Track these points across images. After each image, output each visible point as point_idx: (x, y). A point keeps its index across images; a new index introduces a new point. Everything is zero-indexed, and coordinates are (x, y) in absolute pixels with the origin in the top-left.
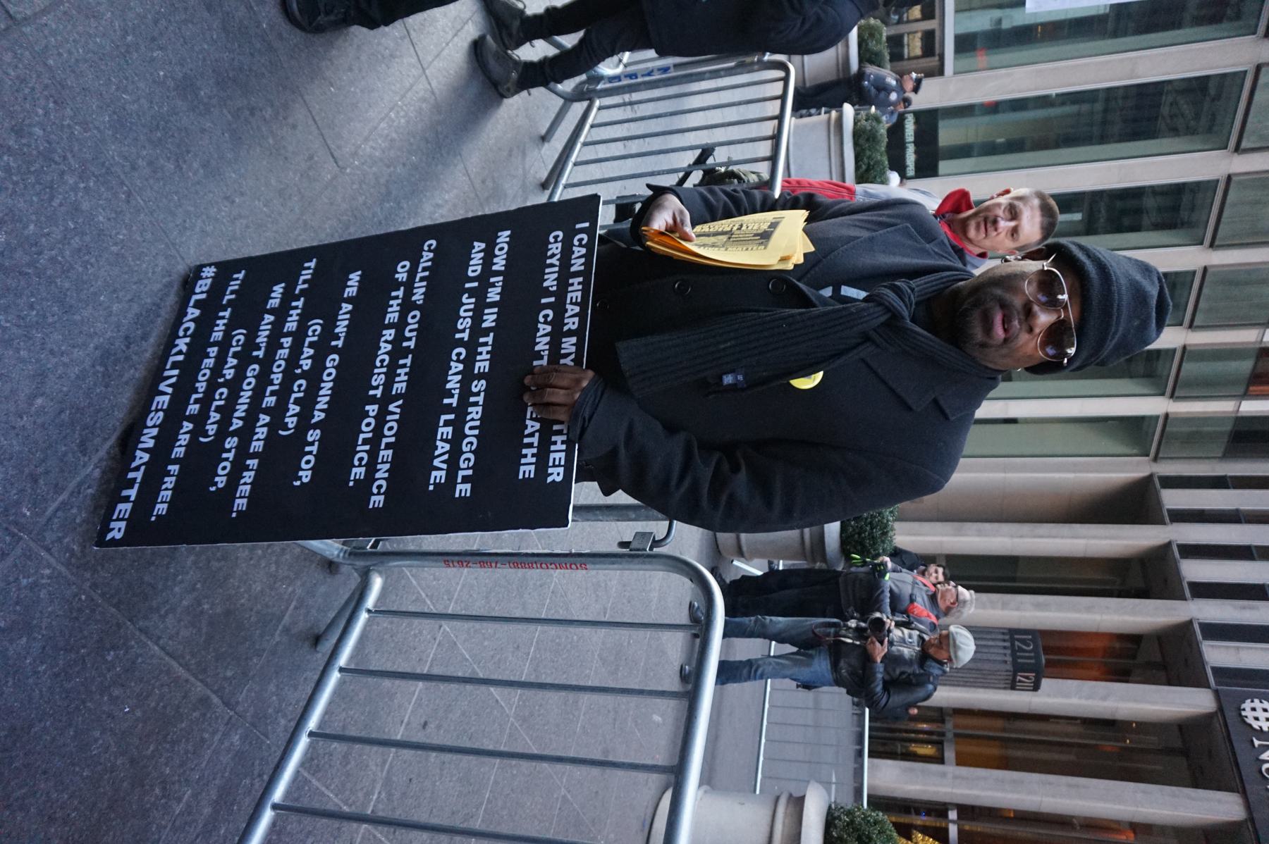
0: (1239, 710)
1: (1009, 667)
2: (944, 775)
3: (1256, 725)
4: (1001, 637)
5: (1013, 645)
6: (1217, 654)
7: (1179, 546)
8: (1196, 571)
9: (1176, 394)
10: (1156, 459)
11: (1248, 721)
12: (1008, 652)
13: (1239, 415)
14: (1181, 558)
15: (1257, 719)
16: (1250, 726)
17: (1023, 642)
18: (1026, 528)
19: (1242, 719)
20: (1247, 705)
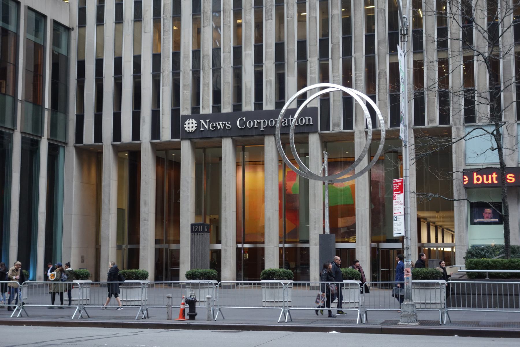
0: (189, 132)
1: (204, 234)
2: (226, 250)
3: (195, 128)
4: (193, 235)
5: (196, 232)
6: (166, 135)
7: (114, 141)
8: (126, 136)
9: (40, 135)
10: (66, 144)
11: (193, 130)
12: (199, 234)
13: (50, 108)
14: (120, 141)
15: (192, 127)
16: (195, 130)
17: (195, 229)
19: (192, 132)
20: (187, 130)
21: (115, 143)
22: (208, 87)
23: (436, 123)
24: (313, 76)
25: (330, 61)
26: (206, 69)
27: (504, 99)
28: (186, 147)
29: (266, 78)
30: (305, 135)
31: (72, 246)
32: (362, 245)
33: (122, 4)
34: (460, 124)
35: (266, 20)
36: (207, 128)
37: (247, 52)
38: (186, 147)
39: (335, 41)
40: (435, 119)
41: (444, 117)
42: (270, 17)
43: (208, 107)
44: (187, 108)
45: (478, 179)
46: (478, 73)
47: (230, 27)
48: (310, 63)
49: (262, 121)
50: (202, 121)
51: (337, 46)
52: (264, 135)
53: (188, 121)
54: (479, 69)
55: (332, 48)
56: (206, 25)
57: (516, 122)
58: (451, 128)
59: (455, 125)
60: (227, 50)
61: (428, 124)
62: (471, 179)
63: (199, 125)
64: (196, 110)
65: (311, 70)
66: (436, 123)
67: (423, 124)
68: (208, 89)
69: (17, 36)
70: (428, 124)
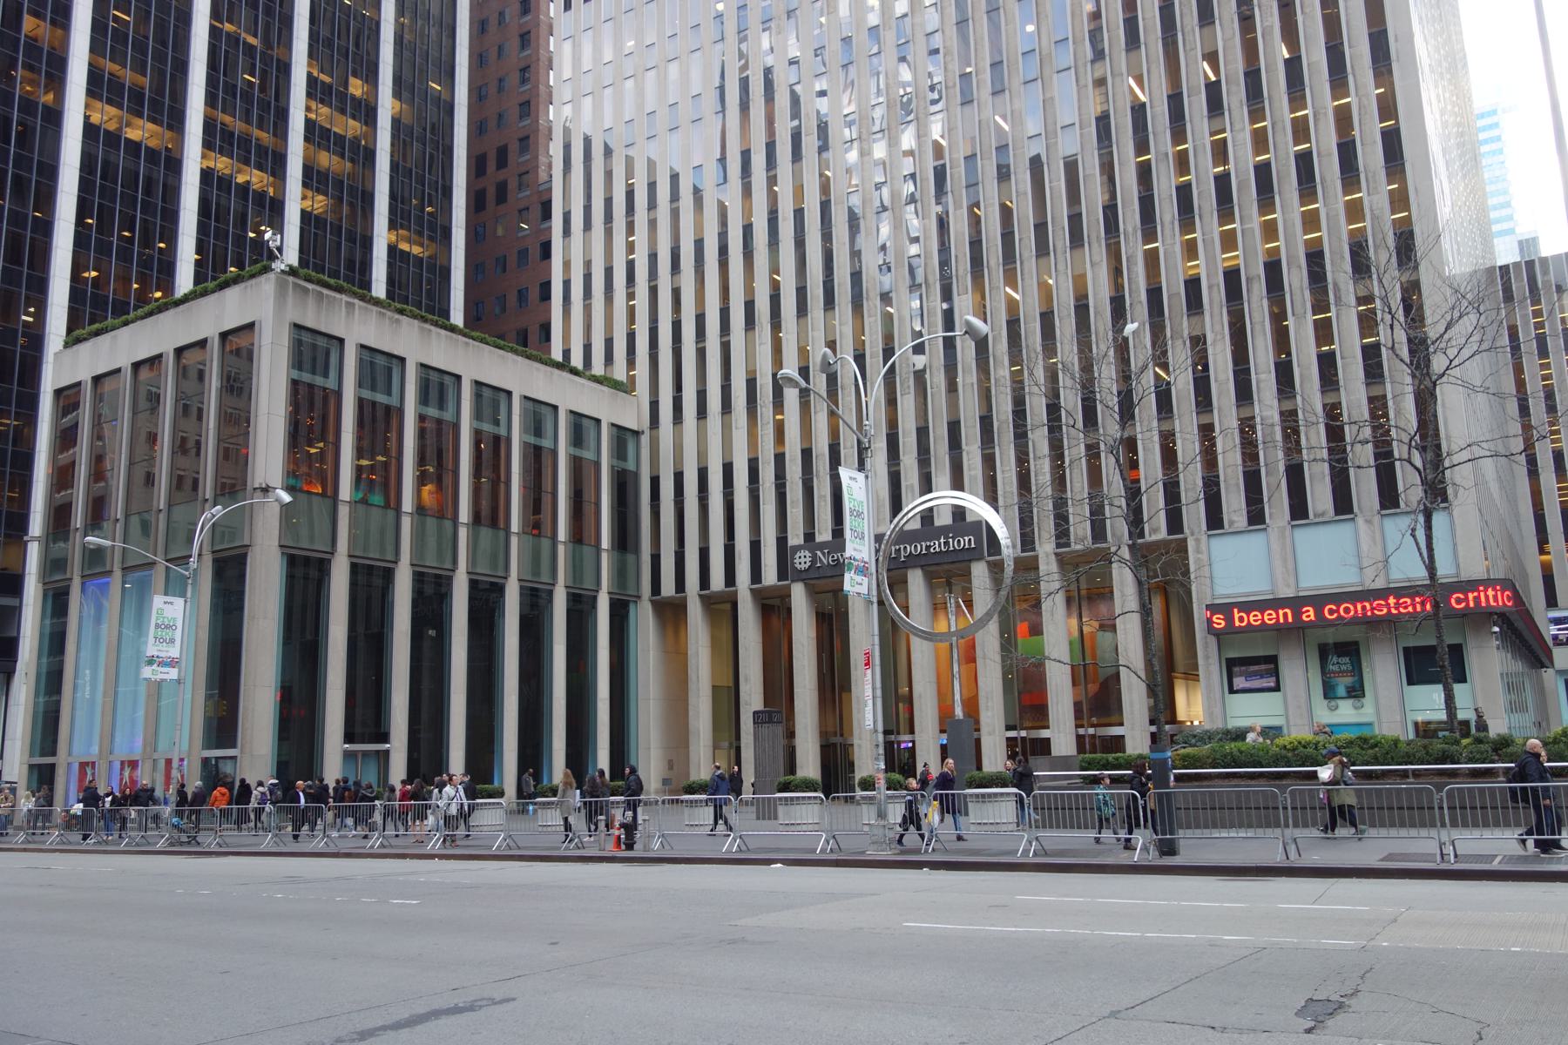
6: (770, 576)
10: (639, 597)
18: (692, 686)
21: (703, 592)
22: (825, 501)
23: (1162, 534)
24: (973, 473)
25: (997, 448)
26: (821, 474)
28: (798, 594)
29: (906, 481)
30: (964, 565)
31: (652, 747)
32: (1059, 732)
33: (658, 401)
34: (1199, 532)
35: (902, 395)
36: (825, 562)
37: (877, 445)
38: (798, 594)
39: (1003, 417)
41: (1175, 522)
42: (907, 391)
43: (826, 530)
44: (797, 535)
45: (1241, 620)
47: (851, 409)
48: (968, 453)
49: (902, 547)
50: (819, 553)
51: (1005, 426)
52: (906, 568)
53: (798, 554)
55: (998, 429)
56: (818, 409)
58: (1185, 540)
60: (849, 444)
61: (1150, 536)
62: (1229, 619)
63: (814, 559)
64: (809, 536)
65: (969, 465)
66: (1162, 534)
68: (826, 505)
69: (554, 453)
70: (1150, 536)
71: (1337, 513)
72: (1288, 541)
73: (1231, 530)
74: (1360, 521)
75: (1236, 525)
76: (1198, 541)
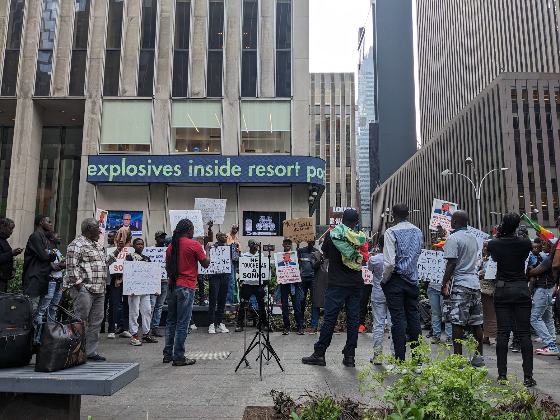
23: (64, 93)
27: (158, 67)
34: (96, 96)
40: (63, 88)
46: (127, 30)
54: (129, 26)
57: (171, 98)
58: (84, 100)
59: (91, 97)
61: (54, 94)
66: (64, 93)
67: (47, 93)
71: (209, 94)
72: (168, 112)
73: (122, 98)
74: (225, 103)
75: (127, 94)
76: (94, 103)
